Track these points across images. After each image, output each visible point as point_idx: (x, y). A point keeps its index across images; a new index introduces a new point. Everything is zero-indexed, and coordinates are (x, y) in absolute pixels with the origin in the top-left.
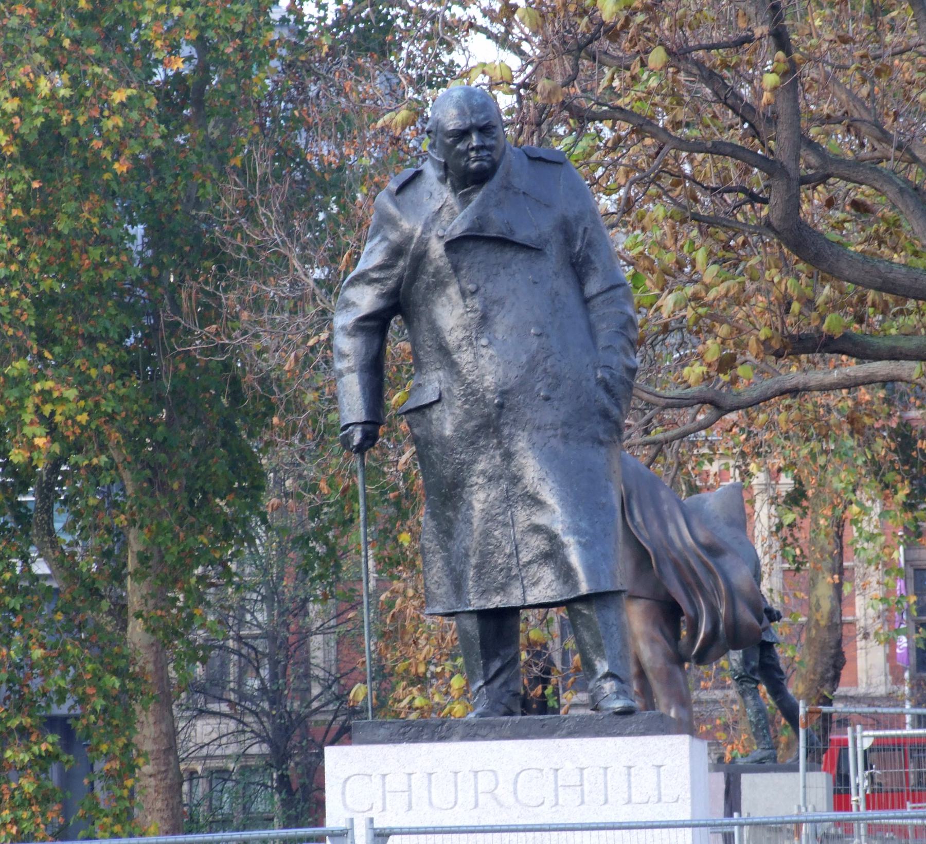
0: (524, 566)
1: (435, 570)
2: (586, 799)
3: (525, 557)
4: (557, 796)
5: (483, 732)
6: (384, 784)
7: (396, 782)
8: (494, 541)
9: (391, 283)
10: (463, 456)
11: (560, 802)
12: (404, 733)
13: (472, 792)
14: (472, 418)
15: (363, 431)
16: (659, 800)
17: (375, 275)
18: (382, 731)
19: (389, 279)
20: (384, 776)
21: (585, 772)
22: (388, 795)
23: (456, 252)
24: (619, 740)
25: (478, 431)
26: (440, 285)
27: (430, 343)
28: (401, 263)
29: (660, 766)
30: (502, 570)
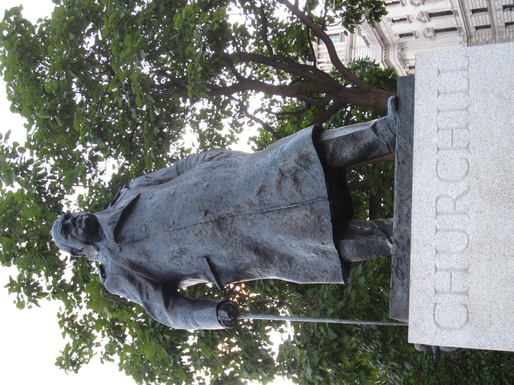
1: (316, 273)
4: (460, 148)
5: (406, 210)
7: (442, 281)
8: (289, 222)
9: (151, 288)
12: (402, 274)
15: (222, 310)
16: (467, 70)
17: (145, 296)
19: (147, 288)
20: (436, 292)
21: (441, 126)
23: (123, 238)
28: (138, 278)
29: (439, 71)
30: (307, 216)
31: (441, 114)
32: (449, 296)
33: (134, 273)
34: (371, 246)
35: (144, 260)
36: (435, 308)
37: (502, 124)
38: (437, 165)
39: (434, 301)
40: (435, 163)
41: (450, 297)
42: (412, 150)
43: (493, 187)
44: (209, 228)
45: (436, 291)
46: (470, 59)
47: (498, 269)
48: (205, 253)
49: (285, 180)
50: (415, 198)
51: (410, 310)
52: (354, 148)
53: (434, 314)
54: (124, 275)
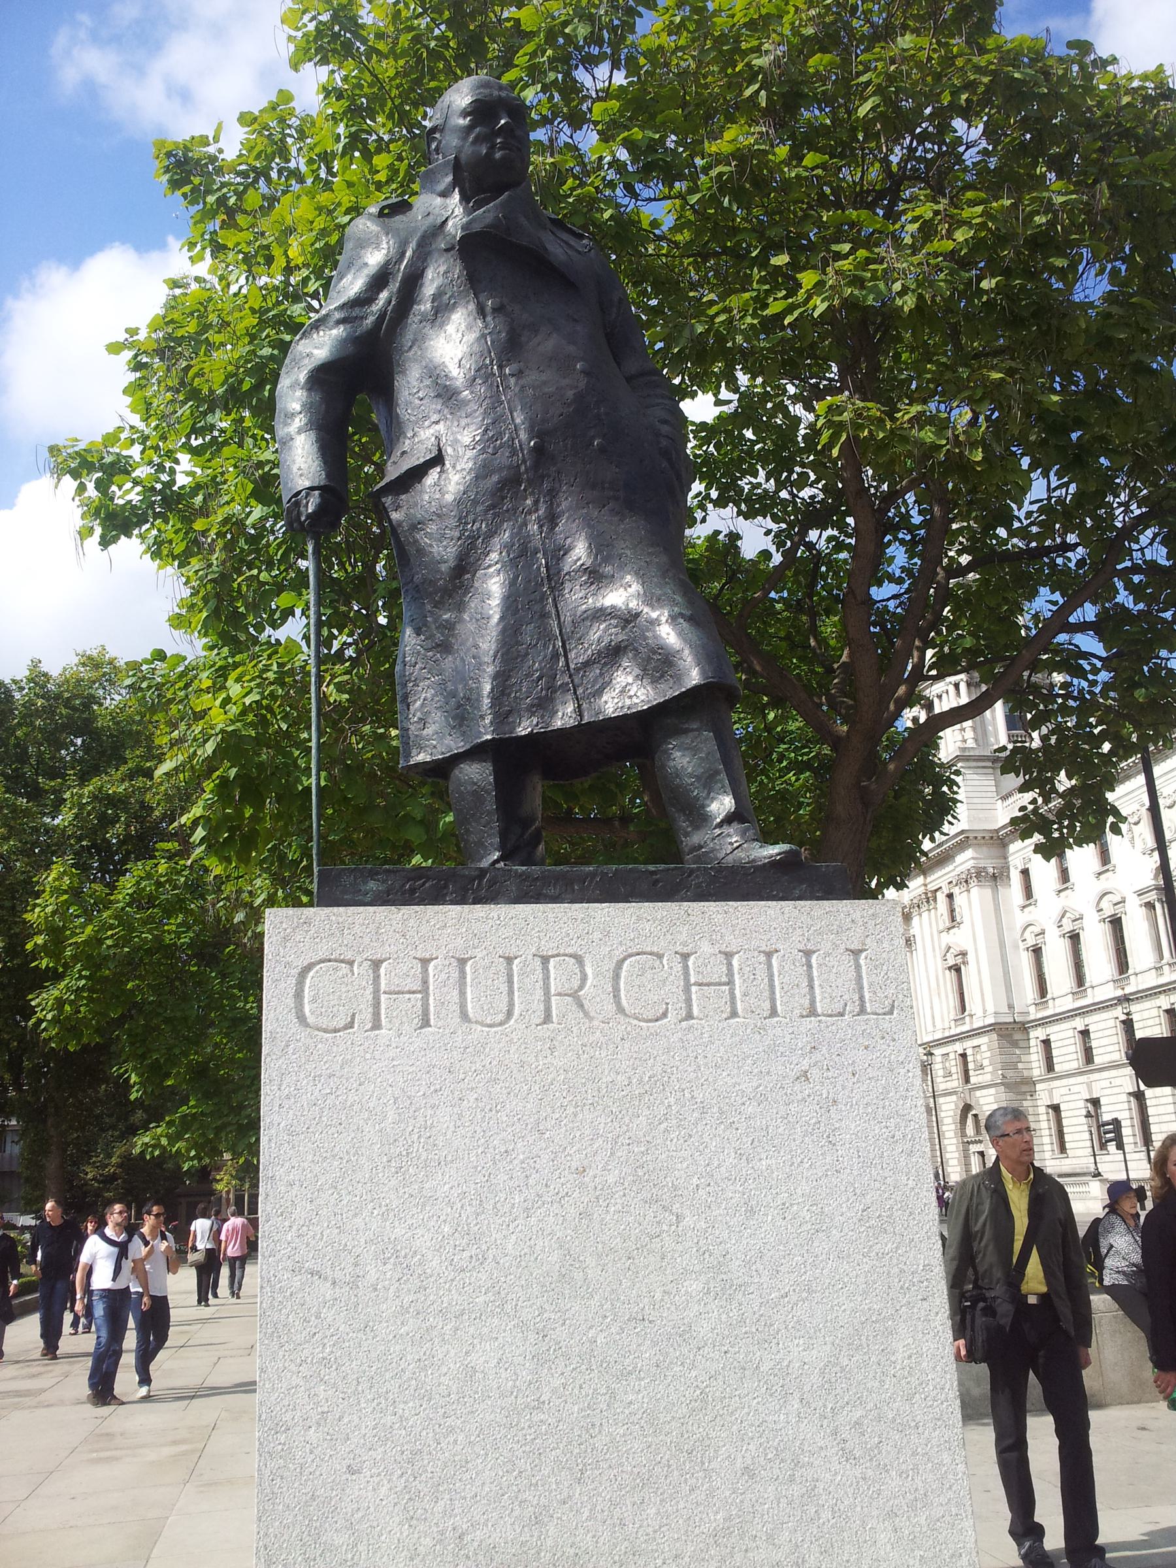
0: (577, 670)
1: (418, 703)
2: (740, 1007)
3: (578, 656)
5: (551, 891)
6: (377, 978)
10: (477, 525)
11: (696, 1012)
12: (413, 891)
13: (539, 993)
14: (492, 472)
18: (372, 885)
22: (383, 997)
24: (788, 905)
25: (501, 489)
26: (441, 310)
27: (421, 394)
28: (384, 295)
29: (861, 951)
31: (762, 958)
32: (370, 989)
33: (394, 286)
34: (483, 821)
35: (425, 306)
36: (342, 961)
37: (743, 1087)
38: (651, 954)
39: (358, 959)
40: (655, 950)
41: (368, 992)
42: (683, 900)
43: (606, 1072)
44: (503, 458)
45: (381, 961)
46: (887, 1017)
47: (432, 1088)
48: (450, 450)
49: (616, 627)
50: (578, 910)
51: (335, 909)
52: (691, 775)
53: (330, 961)
54: (387, 263)
